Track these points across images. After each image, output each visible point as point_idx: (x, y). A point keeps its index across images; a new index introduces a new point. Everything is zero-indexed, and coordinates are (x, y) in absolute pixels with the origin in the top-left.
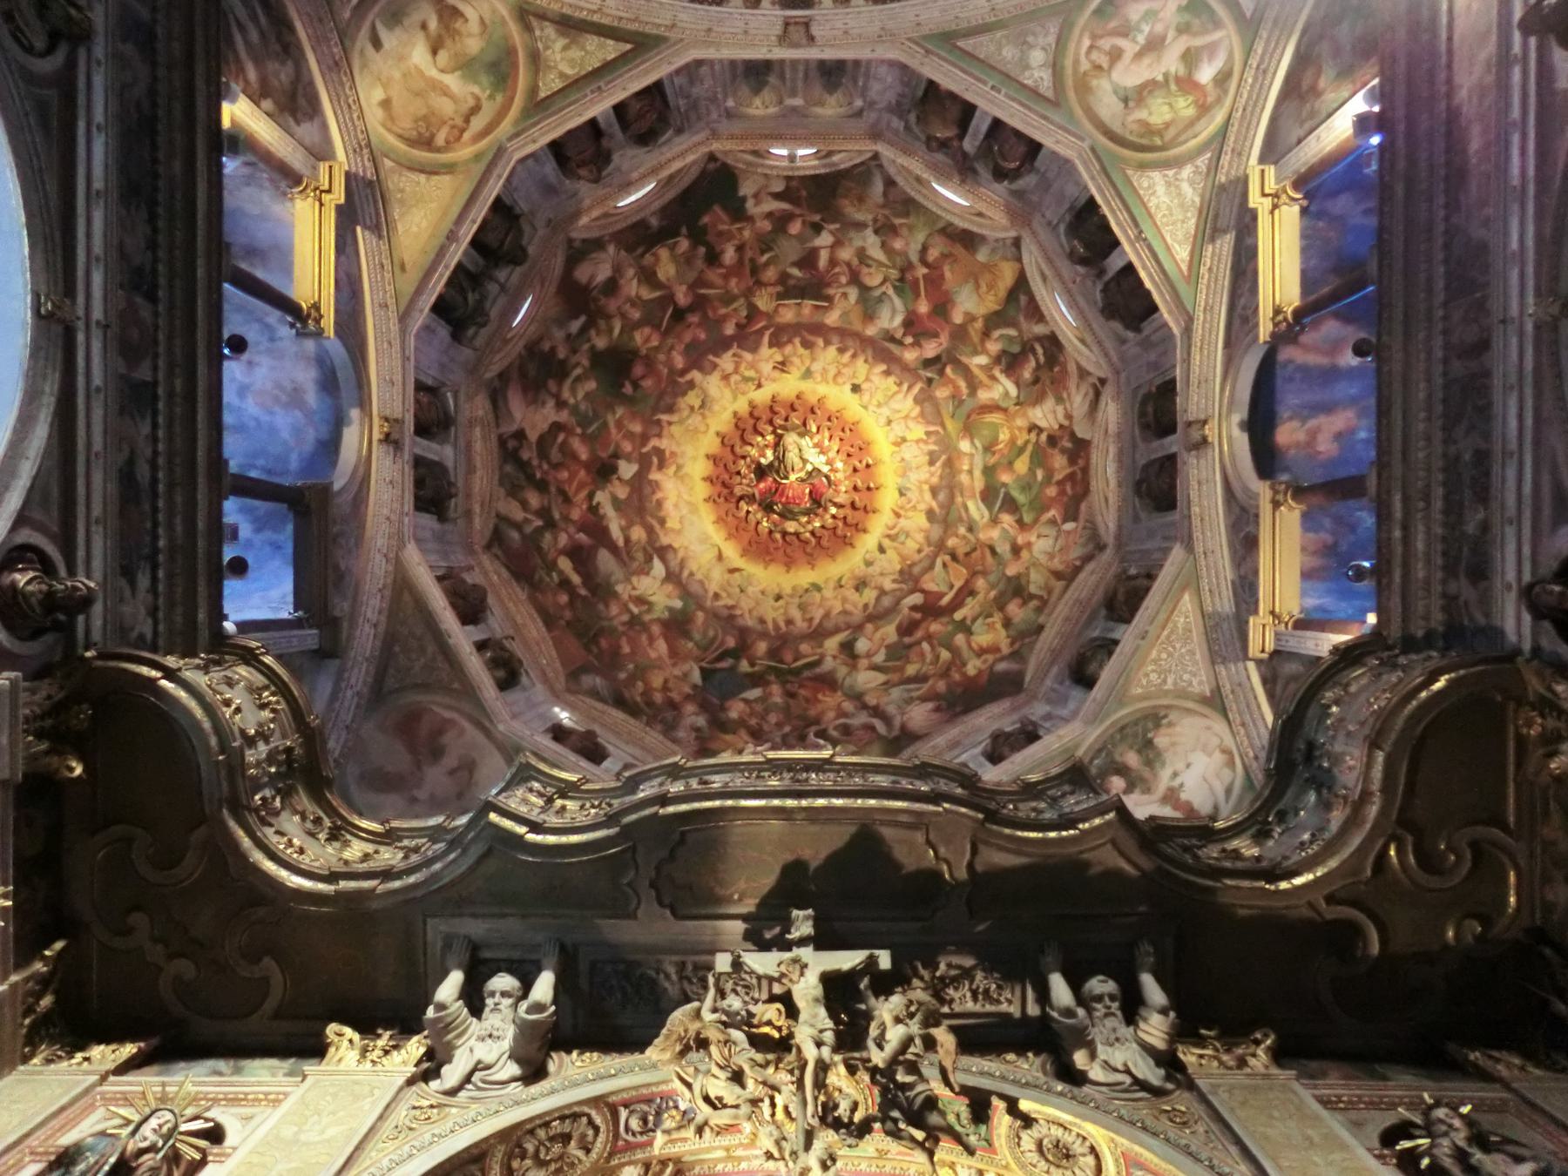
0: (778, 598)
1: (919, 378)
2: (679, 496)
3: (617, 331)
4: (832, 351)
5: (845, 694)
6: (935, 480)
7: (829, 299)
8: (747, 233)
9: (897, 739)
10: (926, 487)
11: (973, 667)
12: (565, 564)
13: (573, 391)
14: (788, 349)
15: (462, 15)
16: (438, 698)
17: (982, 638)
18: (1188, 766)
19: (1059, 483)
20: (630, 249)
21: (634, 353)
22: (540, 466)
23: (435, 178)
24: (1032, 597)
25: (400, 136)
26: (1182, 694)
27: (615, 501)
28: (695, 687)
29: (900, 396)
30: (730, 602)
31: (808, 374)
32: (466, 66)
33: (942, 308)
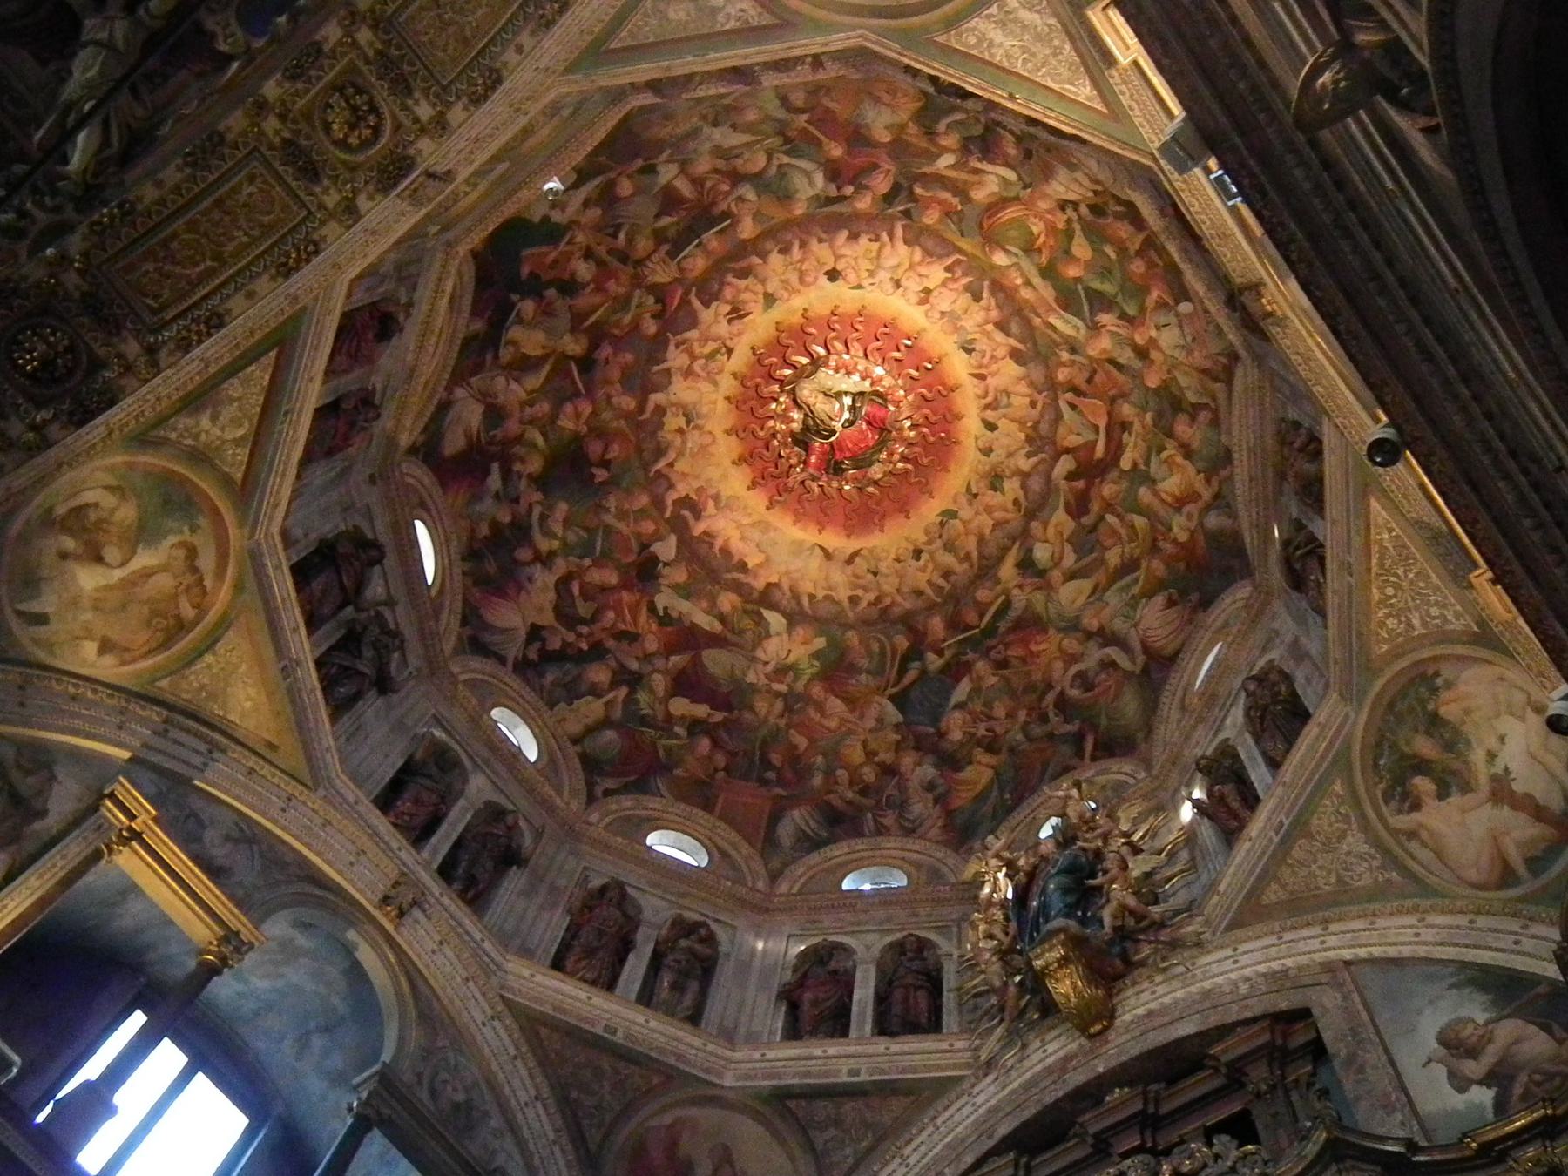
0: (917, 554)
1: (893, 218)
2: (740, 526)
3: (540, 441)
4: (775, 259)
5: (1059, 630)
6: (995, 314)
7: (726, 215)
8: (580, 238)
9: (1146, 671)
10: (990, 327)
11: (1180, 527)
12: (681, 706)
13: (549, 534)
14: (728, 293)
15: (87, 505)
17: (1171, 485)
18: (1502, 739)
19: (1139, 253)
20: (478, 368)
21: (577, 438)
22: (579, 635)
23: (220, 647)
24: (1196, 408)
25: (150, 653)
26: (1446, 638)
27: (676, 588)
28: (897, 726)
29: (888, 248)
30: (871, 596)
31: (770, 299)
32: (143, 534)
33: (857, 138)
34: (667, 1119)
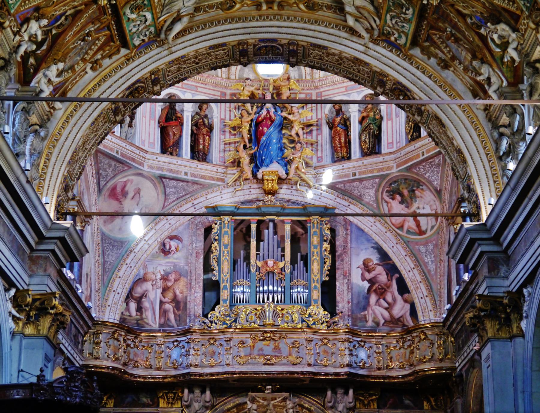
18: (424, 208)
26: (430, 183)
34: (125, 179)
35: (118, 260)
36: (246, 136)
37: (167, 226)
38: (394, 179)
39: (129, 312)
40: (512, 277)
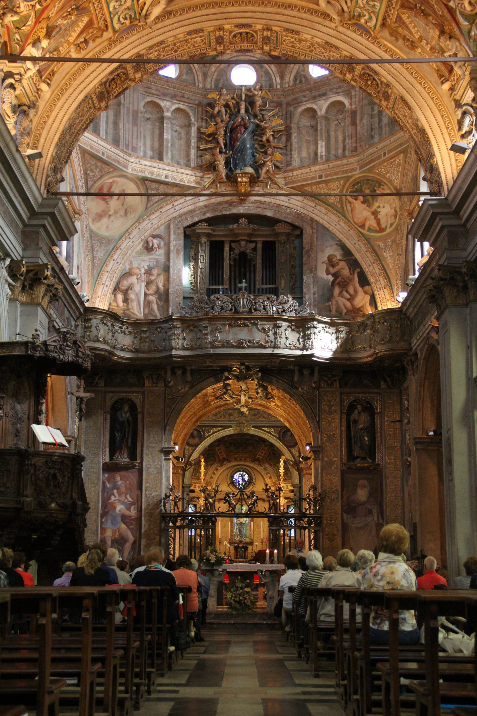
16: (106, 178)
18: (384, 207)
26: (391, 182)
34: (111, 181)
35: (106, 257)
36: (221, 141)
37: (150, 225)
38: (358, 180)
39: (117, 303)
40: (469, 249)
